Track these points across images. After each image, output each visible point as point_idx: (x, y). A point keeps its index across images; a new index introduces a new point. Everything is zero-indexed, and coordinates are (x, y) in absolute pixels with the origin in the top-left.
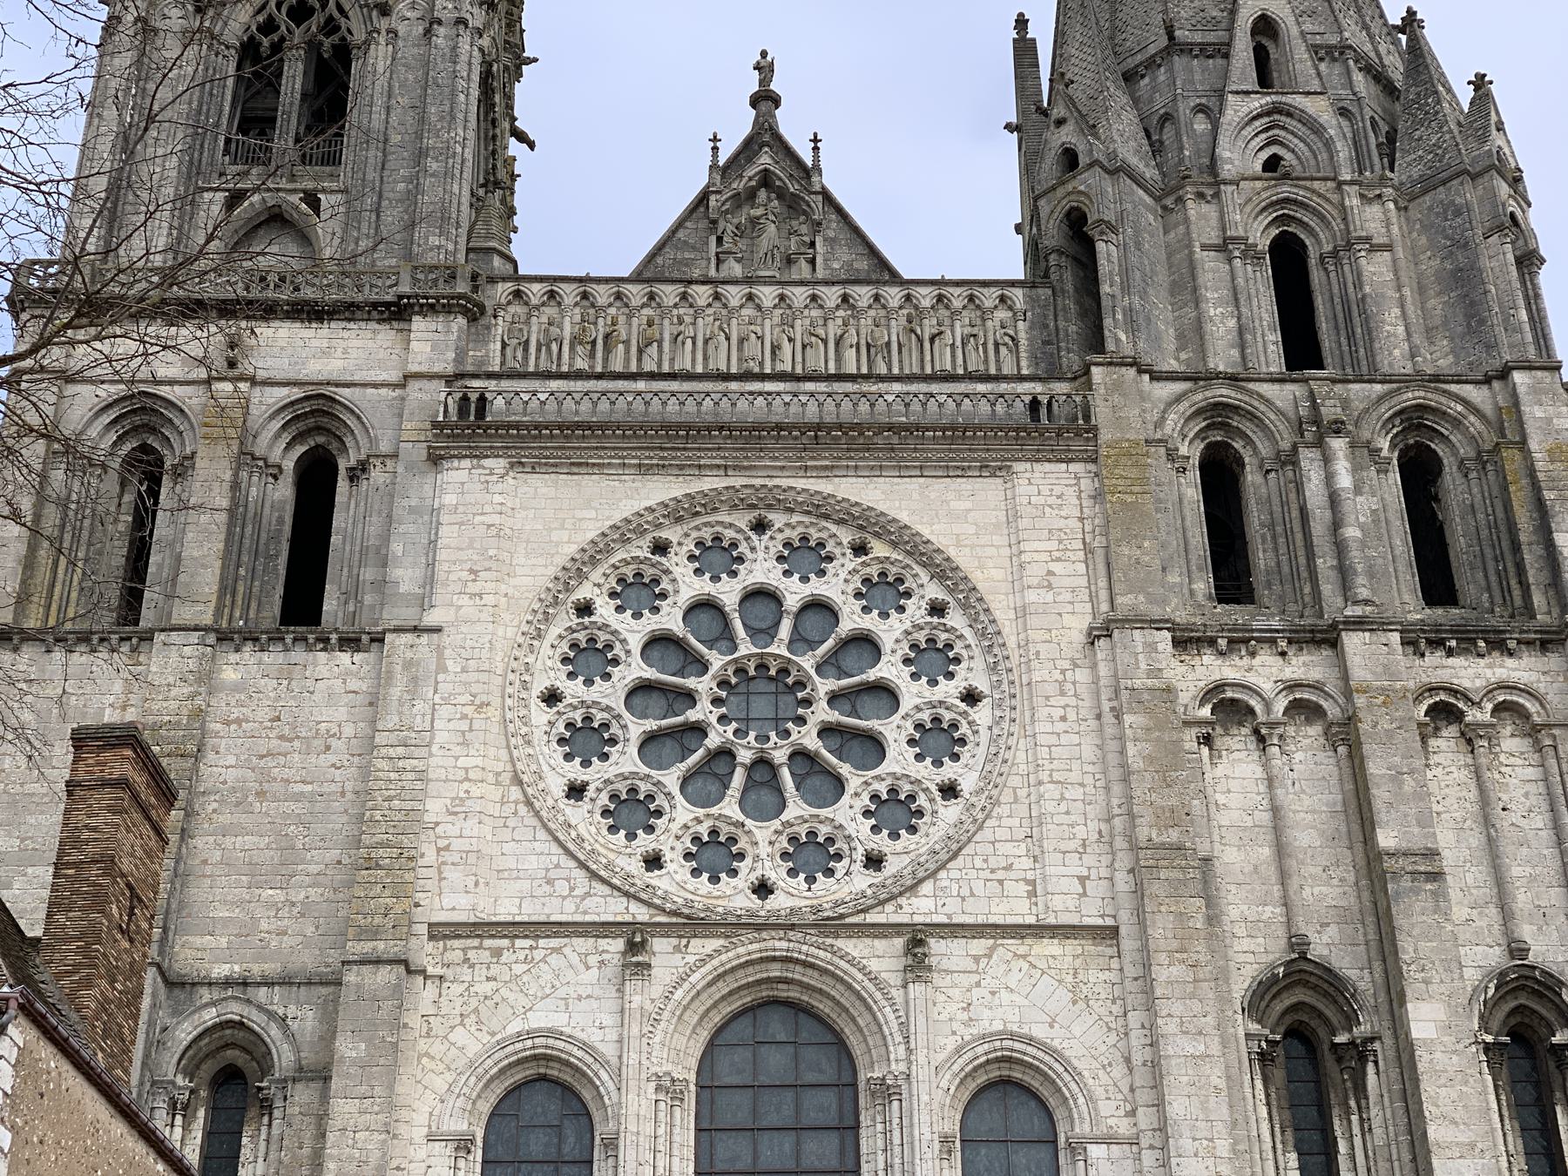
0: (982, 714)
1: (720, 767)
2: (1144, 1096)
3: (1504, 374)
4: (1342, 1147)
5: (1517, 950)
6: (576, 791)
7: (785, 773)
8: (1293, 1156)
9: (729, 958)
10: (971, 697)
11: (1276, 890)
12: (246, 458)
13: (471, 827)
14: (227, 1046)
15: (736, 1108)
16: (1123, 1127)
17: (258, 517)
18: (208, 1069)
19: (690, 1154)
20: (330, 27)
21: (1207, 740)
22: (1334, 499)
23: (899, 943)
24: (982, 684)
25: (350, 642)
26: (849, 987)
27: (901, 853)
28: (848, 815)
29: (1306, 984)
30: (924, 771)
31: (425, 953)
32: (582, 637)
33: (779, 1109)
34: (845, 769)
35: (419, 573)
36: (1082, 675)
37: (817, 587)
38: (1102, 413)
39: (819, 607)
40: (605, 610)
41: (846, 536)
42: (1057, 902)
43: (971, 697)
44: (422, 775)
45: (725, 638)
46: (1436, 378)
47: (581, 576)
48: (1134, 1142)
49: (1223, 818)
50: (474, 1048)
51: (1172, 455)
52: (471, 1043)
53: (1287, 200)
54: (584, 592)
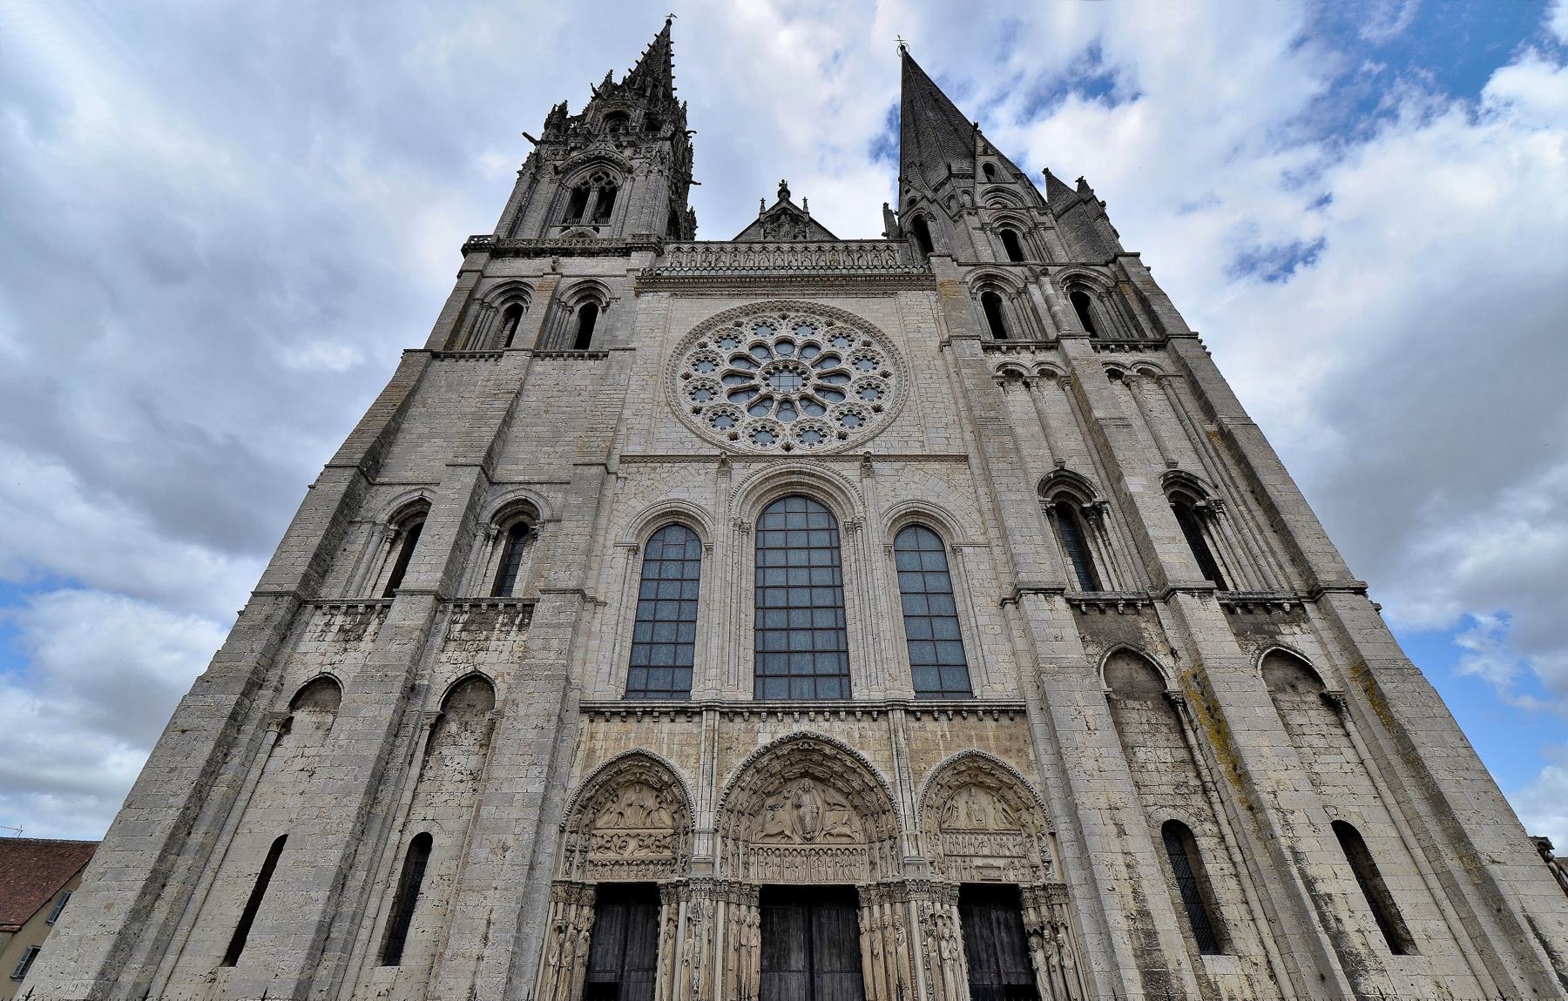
0: (892, 381)
1: (767, 403)
2: (992, 523)
3: (1114, 261)
4: (1095, 555)
5: (1171, 464)
6: (697, 411)
9: (771, 471)
10: (885, 375)
11: (1045, 444)
12: (555, 299)
13: (645, 420)
14: (520, 513)
16: (981, 539)
17: (560, 324)
18: (509, 524)
19: (752, 558)
20: (610, 183)
21: (1002, 384)
22: (1047, 300)
23: (857, 464)
24: (890, 369)
25: (594, 356)
26: (832, 483)
29: (1064, 483)
31: (614, 465)
32: (702, 356)
33: (799, 540)
34: (826, 401)
36: (939, 363)
38: (936, 271)
40: (712, 346)
41: (823, 319)
42: (936, 447)
43: (885, 375)
44: (623, 401)
48: (988, 546)
49: (1014, 417)
50: (640, 508)
52: (639, 505)
53: (1006, 217)
54: (704, 339)
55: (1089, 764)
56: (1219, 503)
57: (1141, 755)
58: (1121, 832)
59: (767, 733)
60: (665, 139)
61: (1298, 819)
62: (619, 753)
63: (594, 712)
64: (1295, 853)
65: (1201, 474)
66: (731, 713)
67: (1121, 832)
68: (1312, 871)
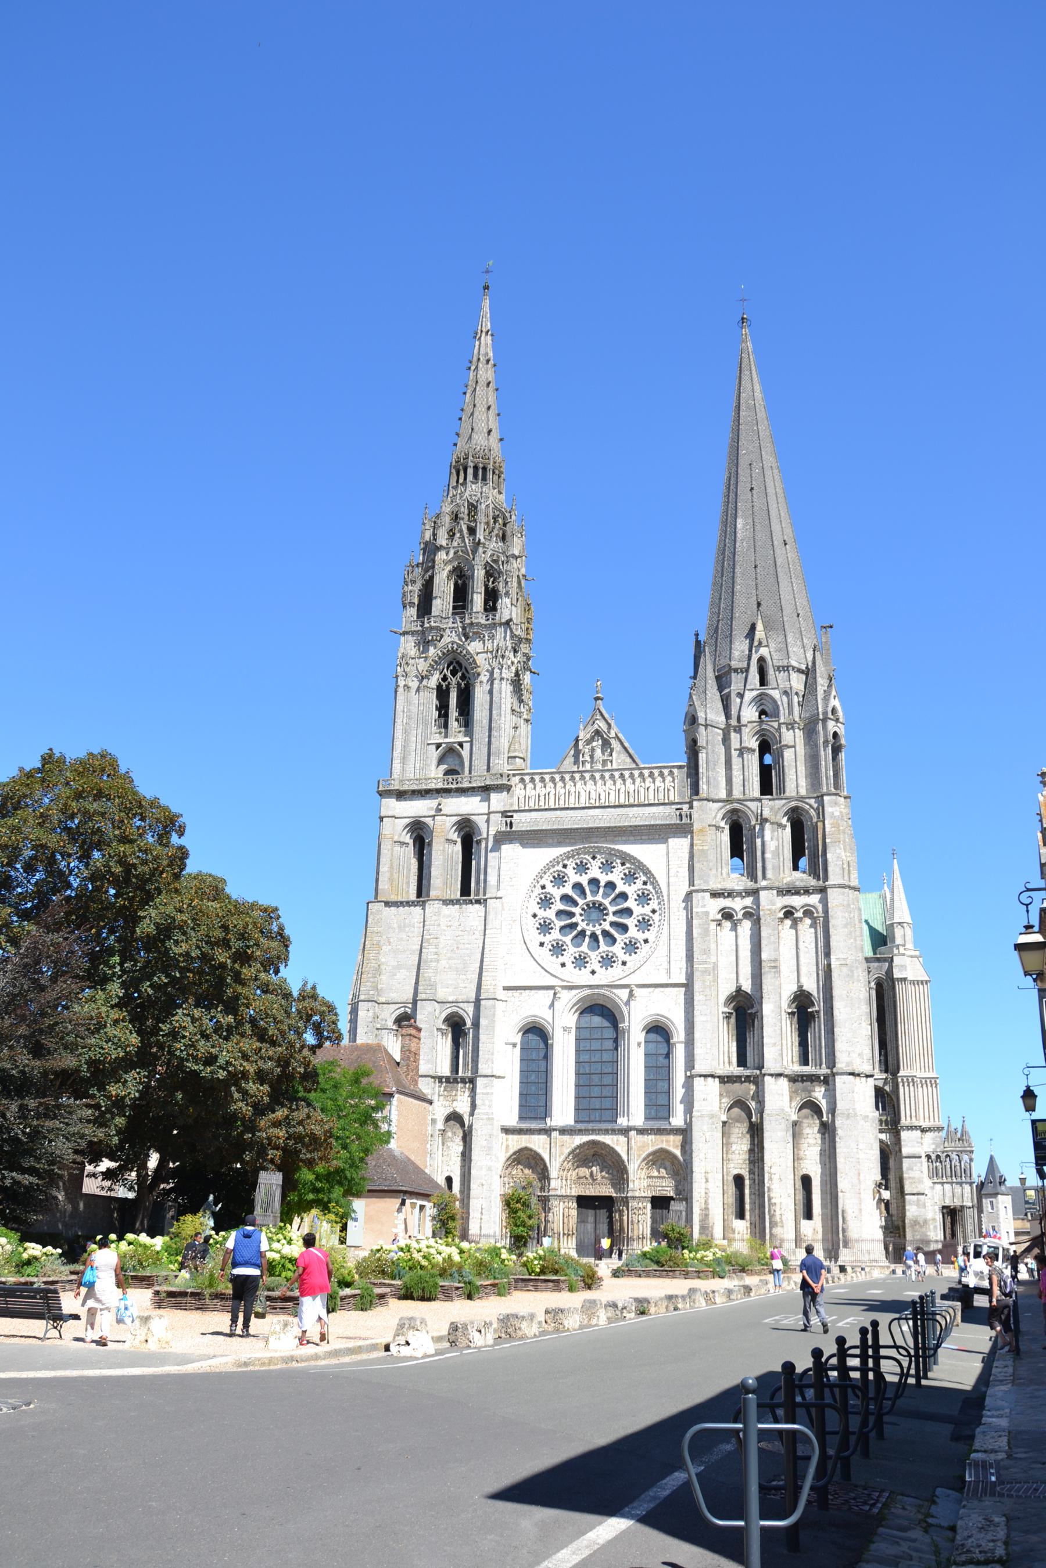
0: (656, 917)
3: (822, 796)
5: (800, 987)
7: (601, 938)
8: (735, 1044)
10: (654, 911)
15: (586, 1034)
24: (657, 908)
25: (478, 902)
27: (632, 960)
28: (617, 949)
30: (640, 936)
32: (543, 896)
34: (616, 935)
35: (496, 878)
37: (611, 877)
38: (695, 816)
39: (610, 885)
43: (654, 911)
45: (583, 893)
46: (802, 797)
47: (541, 877)
51: (718, 828)
54: (542, 882)
55: (702, 1156)
56: (818, 1012)
57: (734, 1147)
58: (707, 1181)
59: (579, 1140)
60: (501, 624)
61: (775, 1178)
62: (519, 1147)
63: (506, 1130)
64: (769, 1188)
65: (815, 994)
66: (563, 1131)
67: (707, 1181)
68: (772, 1195)
